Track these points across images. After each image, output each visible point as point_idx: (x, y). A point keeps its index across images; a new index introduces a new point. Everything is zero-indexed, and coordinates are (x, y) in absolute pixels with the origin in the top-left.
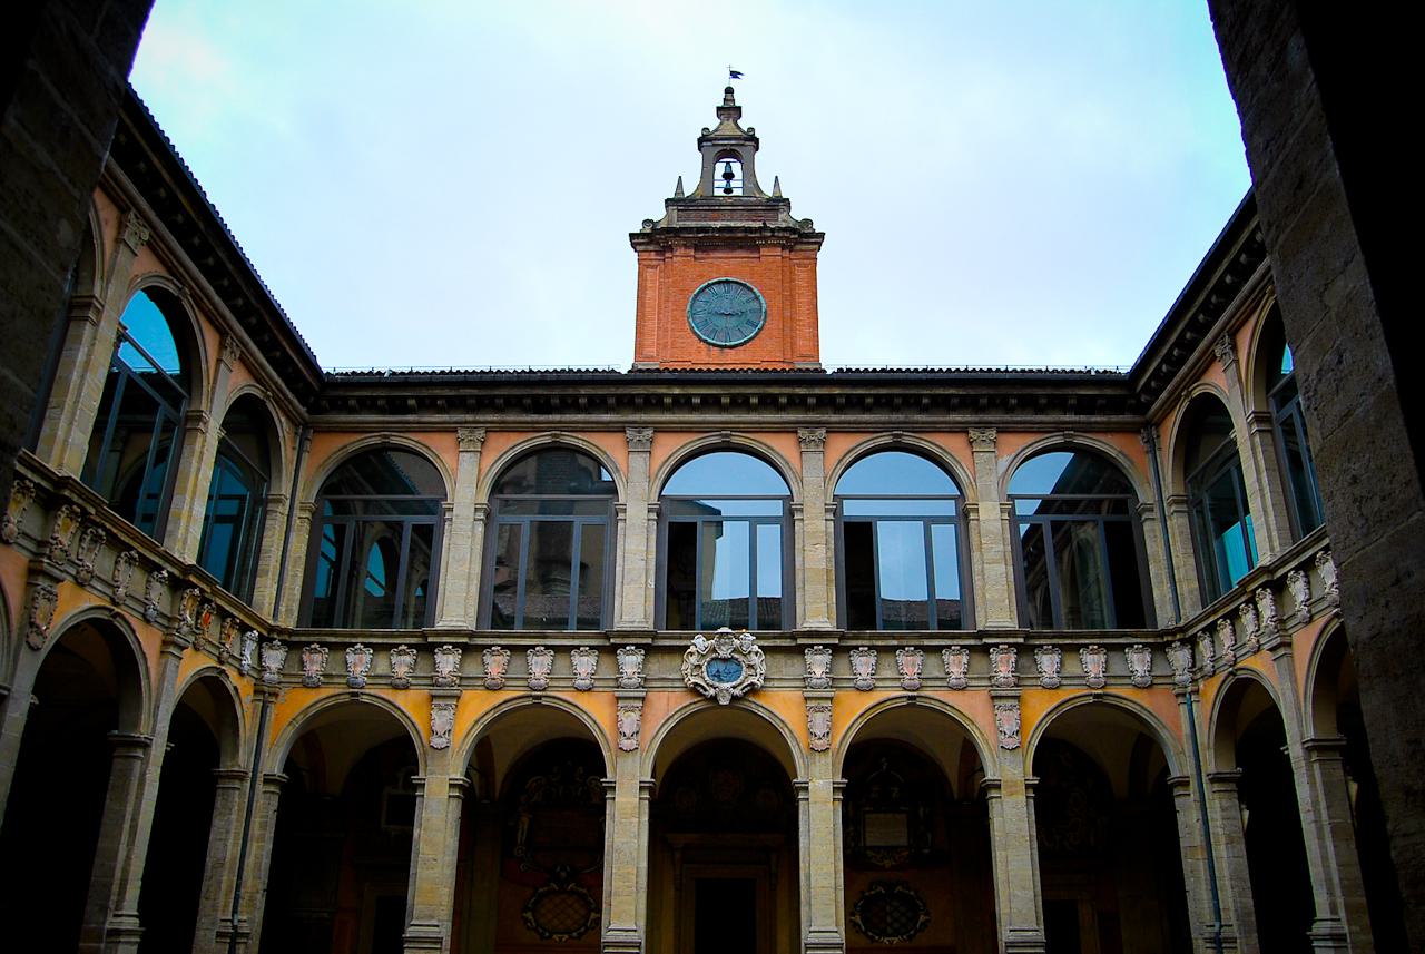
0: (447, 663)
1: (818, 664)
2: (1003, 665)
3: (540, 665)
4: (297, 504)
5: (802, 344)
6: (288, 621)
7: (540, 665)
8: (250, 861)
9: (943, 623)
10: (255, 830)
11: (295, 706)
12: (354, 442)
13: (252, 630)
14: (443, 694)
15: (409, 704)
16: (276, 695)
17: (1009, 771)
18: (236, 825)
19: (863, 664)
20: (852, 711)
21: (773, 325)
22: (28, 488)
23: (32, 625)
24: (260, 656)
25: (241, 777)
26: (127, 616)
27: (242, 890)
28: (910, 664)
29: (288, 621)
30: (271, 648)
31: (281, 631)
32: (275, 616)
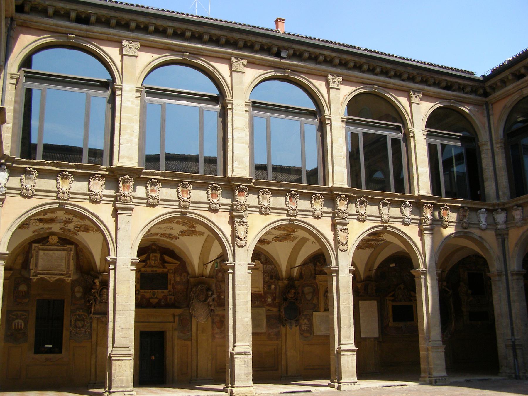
4: (494, 142)
6: (504, 199)
8: (513, 312)
10: (513, 297)
12: (509, 102)
13: (480, 209)
16: (507, 234)
18: (504, 297)
22: (319, 197)
23: (339, 243)
24: (494, 218)
25: (500, 275)
26: (393, 225)
27: (514, 325)
29: (504, 199)
30: (498, 213)
31: (498, 205)
32: (498, 197)
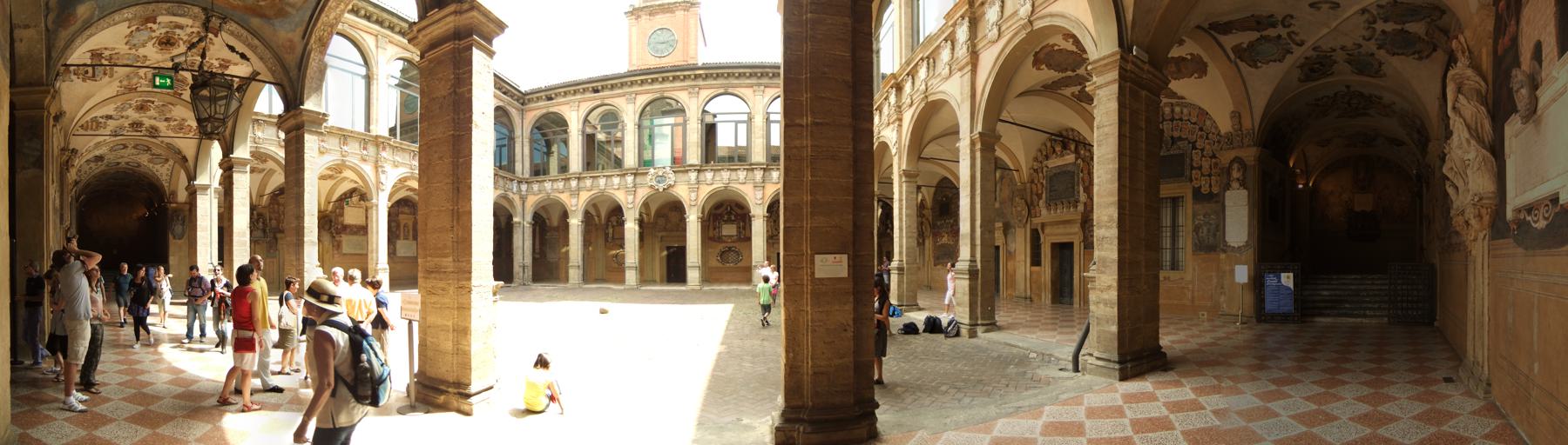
0: (574, 183)
1: (693, 175)
2: (759, 175)
3: (602, 181)
5: (692, 53)
6: (527, 175)
7: (602, 181)
9: (738, 158)
11: (532, 201)
14: (576, 193)
15: (564, 197)
17: (758, 212)
19: (709, 175)
20: (705, 191)
21: (680, 46)
28: (725, 175)
